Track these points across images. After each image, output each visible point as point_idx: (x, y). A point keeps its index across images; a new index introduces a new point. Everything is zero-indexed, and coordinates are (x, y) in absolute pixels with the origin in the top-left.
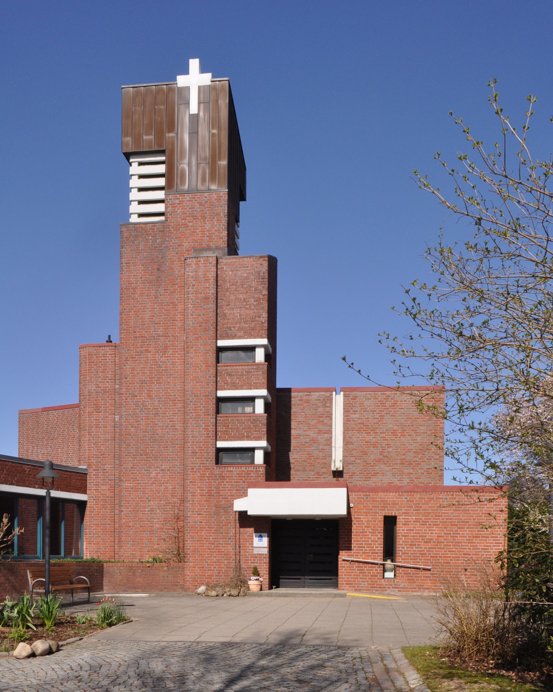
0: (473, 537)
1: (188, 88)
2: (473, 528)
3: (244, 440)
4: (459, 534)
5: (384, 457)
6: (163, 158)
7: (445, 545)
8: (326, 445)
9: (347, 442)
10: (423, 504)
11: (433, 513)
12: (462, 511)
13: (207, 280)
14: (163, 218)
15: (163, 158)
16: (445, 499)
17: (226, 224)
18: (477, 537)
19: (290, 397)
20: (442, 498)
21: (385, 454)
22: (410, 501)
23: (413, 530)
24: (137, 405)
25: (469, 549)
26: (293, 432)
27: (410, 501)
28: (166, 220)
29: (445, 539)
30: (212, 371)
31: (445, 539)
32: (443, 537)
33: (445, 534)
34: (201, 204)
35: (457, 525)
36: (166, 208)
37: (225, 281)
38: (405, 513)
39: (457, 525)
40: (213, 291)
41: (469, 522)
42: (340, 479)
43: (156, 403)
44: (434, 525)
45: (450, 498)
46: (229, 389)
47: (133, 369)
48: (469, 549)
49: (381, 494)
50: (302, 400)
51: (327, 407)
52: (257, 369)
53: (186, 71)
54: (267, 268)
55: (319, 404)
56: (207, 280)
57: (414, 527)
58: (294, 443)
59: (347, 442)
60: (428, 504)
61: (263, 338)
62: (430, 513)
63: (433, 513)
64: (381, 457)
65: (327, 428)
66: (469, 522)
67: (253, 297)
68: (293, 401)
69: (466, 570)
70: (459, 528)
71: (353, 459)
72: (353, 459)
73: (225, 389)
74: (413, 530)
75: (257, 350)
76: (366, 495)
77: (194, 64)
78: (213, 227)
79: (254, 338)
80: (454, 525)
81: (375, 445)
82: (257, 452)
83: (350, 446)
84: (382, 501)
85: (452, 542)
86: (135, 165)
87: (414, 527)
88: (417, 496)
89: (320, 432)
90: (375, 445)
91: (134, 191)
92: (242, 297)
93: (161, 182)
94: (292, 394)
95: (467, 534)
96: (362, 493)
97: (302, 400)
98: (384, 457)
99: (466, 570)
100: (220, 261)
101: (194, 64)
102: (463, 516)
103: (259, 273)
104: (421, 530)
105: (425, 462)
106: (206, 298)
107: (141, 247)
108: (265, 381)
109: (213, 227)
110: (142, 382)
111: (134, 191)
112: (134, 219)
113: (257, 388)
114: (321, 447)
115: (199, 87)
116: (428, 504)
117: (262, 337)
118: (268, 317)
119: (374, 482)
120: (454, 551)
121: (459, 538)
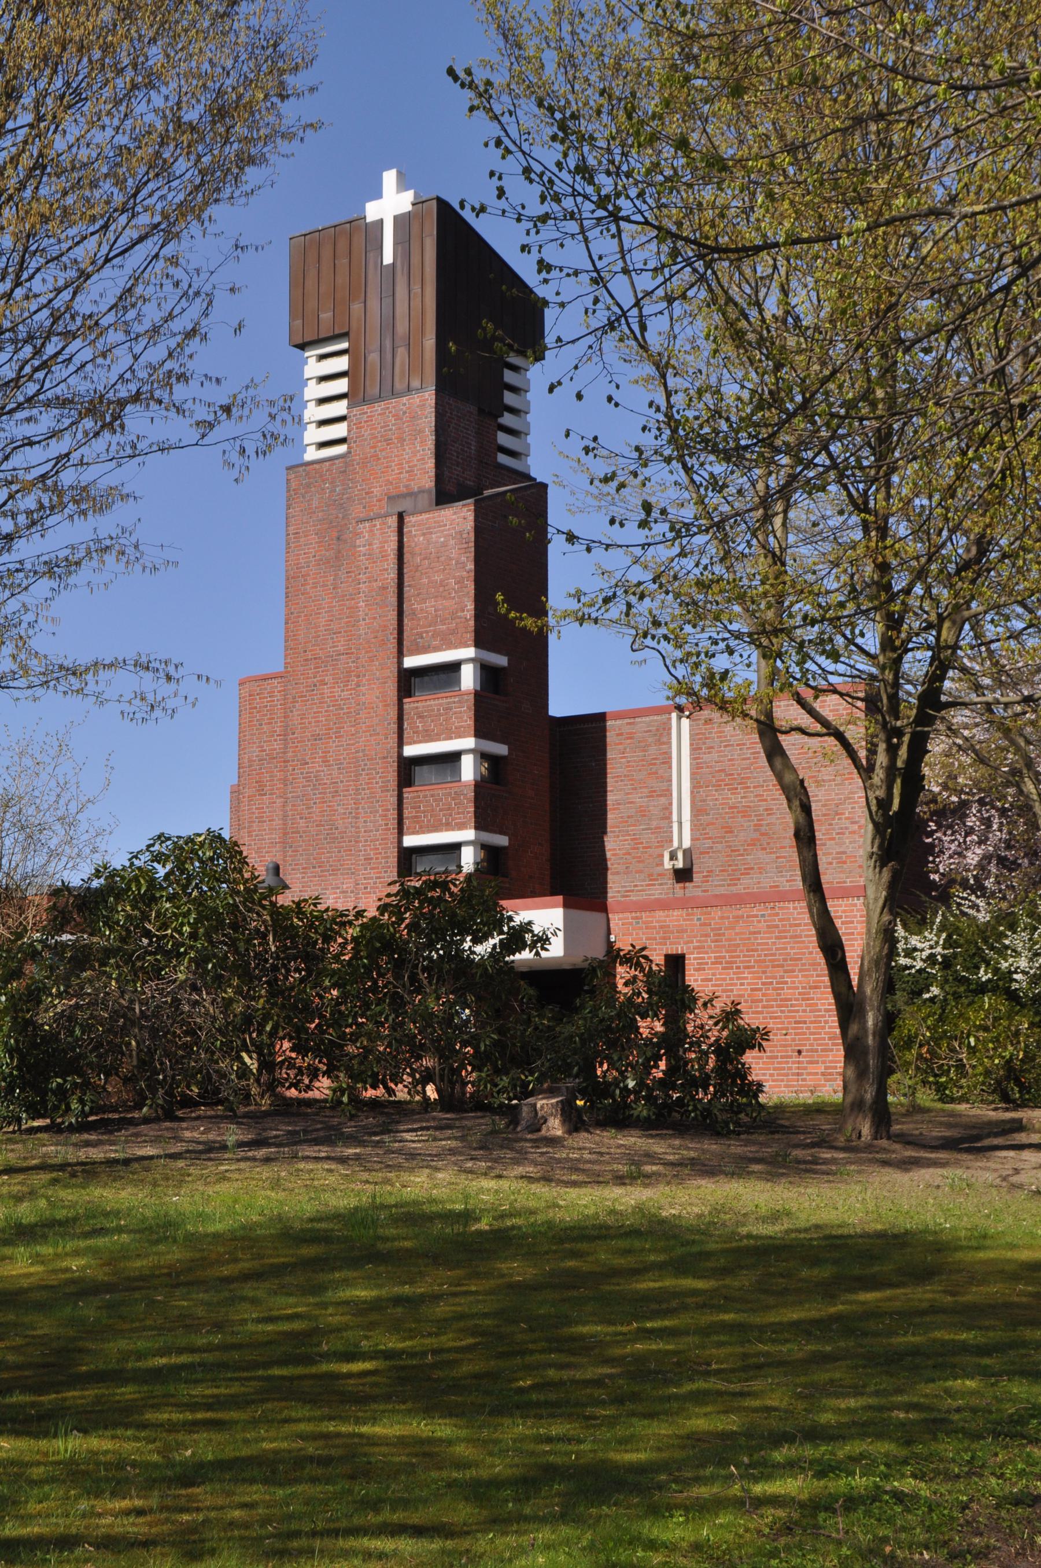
0: (811, 988)
1: (381, 222)
2: (808, 970)
3: (441, 830)
4: (786, 983)
5: (762, 834)
6: (345, 345)
7: (764, 1007)
8: (663, 819)
9: (699, 811)
10: (727, 929)
11: (744, 945)
12: (791, 937)
13: (384, 556)
14: (341, 449)
15: (345, 345)
16: (763, 916)
17: (433, 447)
18: (816, 987)
19: (604, 730)
20: (756, 916)
21: (763, 829)
22: (705, 924)
23: (711, 980)
24: (308, 779)
25: (804, 1011)
26: (611, 798)
27: (705, 924)
28: (349, 452)
29: (764, 995)
30: (393, 713)
31: (764, 995)
32: (760, 989)
33: (763, 984)
34: (397, 417)
35: (782, 966)
36: (349, 431)
37: (413, 554)
38: (698, 947)
39: (782, 966)
40: (393, 575)
41: (801, 959)
42: (687, 884)
43: (335, 773)
44: (745, 967)
45: (770, 915)
46: (420, 742)
47: (303, 716)
48: (804, 1011)
49: (660, 914)
50: (621, 734)
51: (664, 743)
52: (459, 702)
53: (377, 194)
54: (472, 524)
55: (650, 740)
56: (384, 556)
57: (714, 974)
58: (611, 817)
59: (697, 811)
60: (733, 928)
61: (468, 646)
62: (738, 945)
63: (744, 945)
64: (756, 835)
65: (664, 786)
66: (801, 959)
67: (454, 577)
68: (611, 737)
69: (799, 1052)
70: (786, 971)
71: (708, 843)
72: (708, 843)
73: (415, 742)
74: (711, 980)
75: (463, 667)
76: (637, 918)
77: (390, 178)
78: (414, 454)
79: (456, 648)
80: (778, 966)
81: (745, 813)
82: (464, 849)
83: (704, 819)
84: (661, 927)
85: (776, 1000)
86: (312, 361)
87: (714, 974)
88: (717, 913)
89: (652, 794)
90: (745, 813)
91: (311, 405)
92: (437, 578)
93: (341, 386)
94: (609, 723)
95: (800, 982)
96: (628, 915)
97: (621, 734)
98: (762, 834)
99: (799, 1052)
100: (407, 519)
101: (390, 178)
102: (792, 948)
103: (461, 533)
104: (724, 979)
105: (833, 839)
106: (385, 588)
107: (315, 503)
108: (471, 723)
109: (414, 454)
110: (316, 737)
111: (311, 405)
112: (312, 454)
113: (460, 737)
114: (654, 824)
115: (396, 218)
116: (733, 928)
117: (465, 645)
118: (476, 609)
119: (747, 884)
120: (779, 1017)
121: (786, 992)
